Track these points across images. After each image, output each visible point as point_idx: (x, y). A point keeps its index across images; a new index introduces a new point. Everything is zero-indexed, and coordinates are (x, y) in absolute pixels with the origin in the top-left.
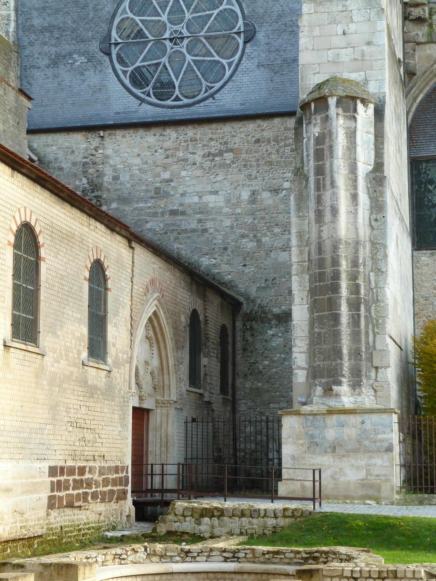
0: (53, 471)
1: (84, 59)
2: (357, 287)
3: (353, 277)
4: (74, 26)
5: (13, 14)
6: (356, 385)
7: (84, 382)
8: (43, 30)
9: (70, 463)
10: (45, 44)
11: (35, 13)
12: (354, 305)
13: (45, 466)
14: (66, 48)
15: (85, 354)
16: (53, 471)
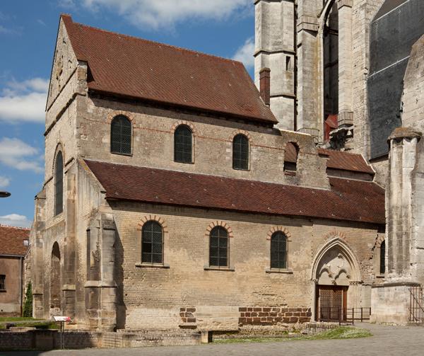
0: (241, 309)
1: (391, 121)
2: (402, 227)
3: (400, 223)
4: (387, 105)
5: (365, 106)
6: (400, 272)
7: (269, 278)
8: (377, 110)
9: (257, 307)
10: (378, 117)
11: (374, 103)
12: (400, 236)
13: (237, 308)
14: (385, 117)
15: (268, 267)
16: (241, 309)
